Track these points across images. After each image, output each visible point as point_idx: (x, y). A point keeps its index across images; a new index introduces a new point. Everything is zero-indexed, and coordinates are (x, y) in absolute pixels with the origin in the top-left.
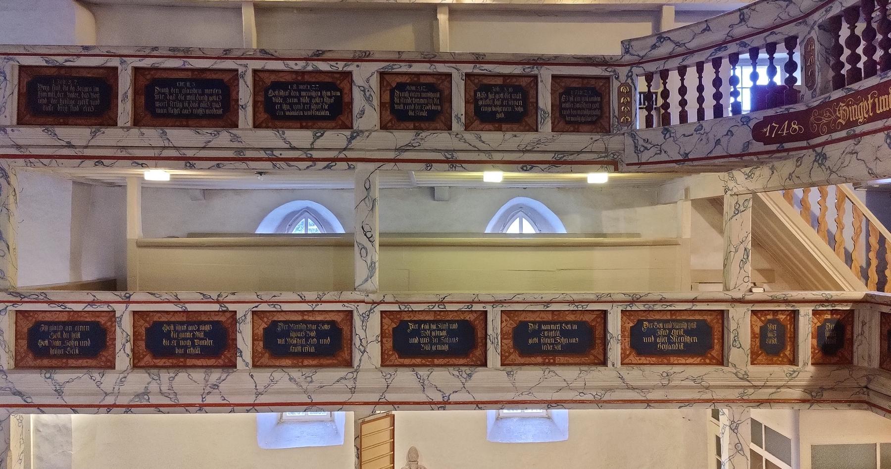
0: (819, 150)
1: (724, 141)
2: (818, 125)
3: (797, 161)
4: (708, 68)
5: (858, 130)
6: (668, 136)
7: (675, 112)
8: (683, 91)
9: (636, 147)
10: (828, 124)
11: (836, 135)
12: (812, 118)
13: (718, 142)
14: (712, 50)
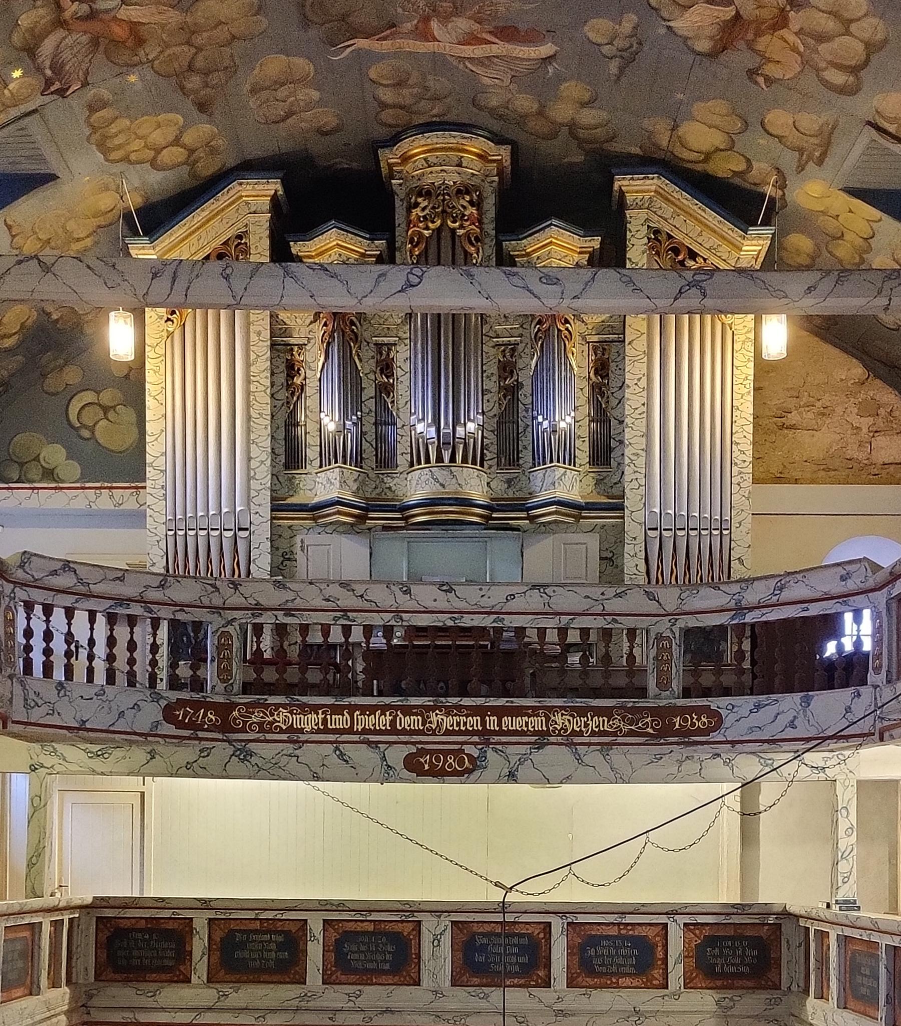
0: (238, 745)
1: (129, 714)
2: (245, 722)
3: (201, 751)
4: (101, 620)
5: (303, 737)
6: (62, 692)
7: (37, 658)
8: (48, 636)
9: (26, 700)
10: (261, 724)
11: (269, 736)
12: (235, 713)
13: (121, 714)
14: (111, 602)
